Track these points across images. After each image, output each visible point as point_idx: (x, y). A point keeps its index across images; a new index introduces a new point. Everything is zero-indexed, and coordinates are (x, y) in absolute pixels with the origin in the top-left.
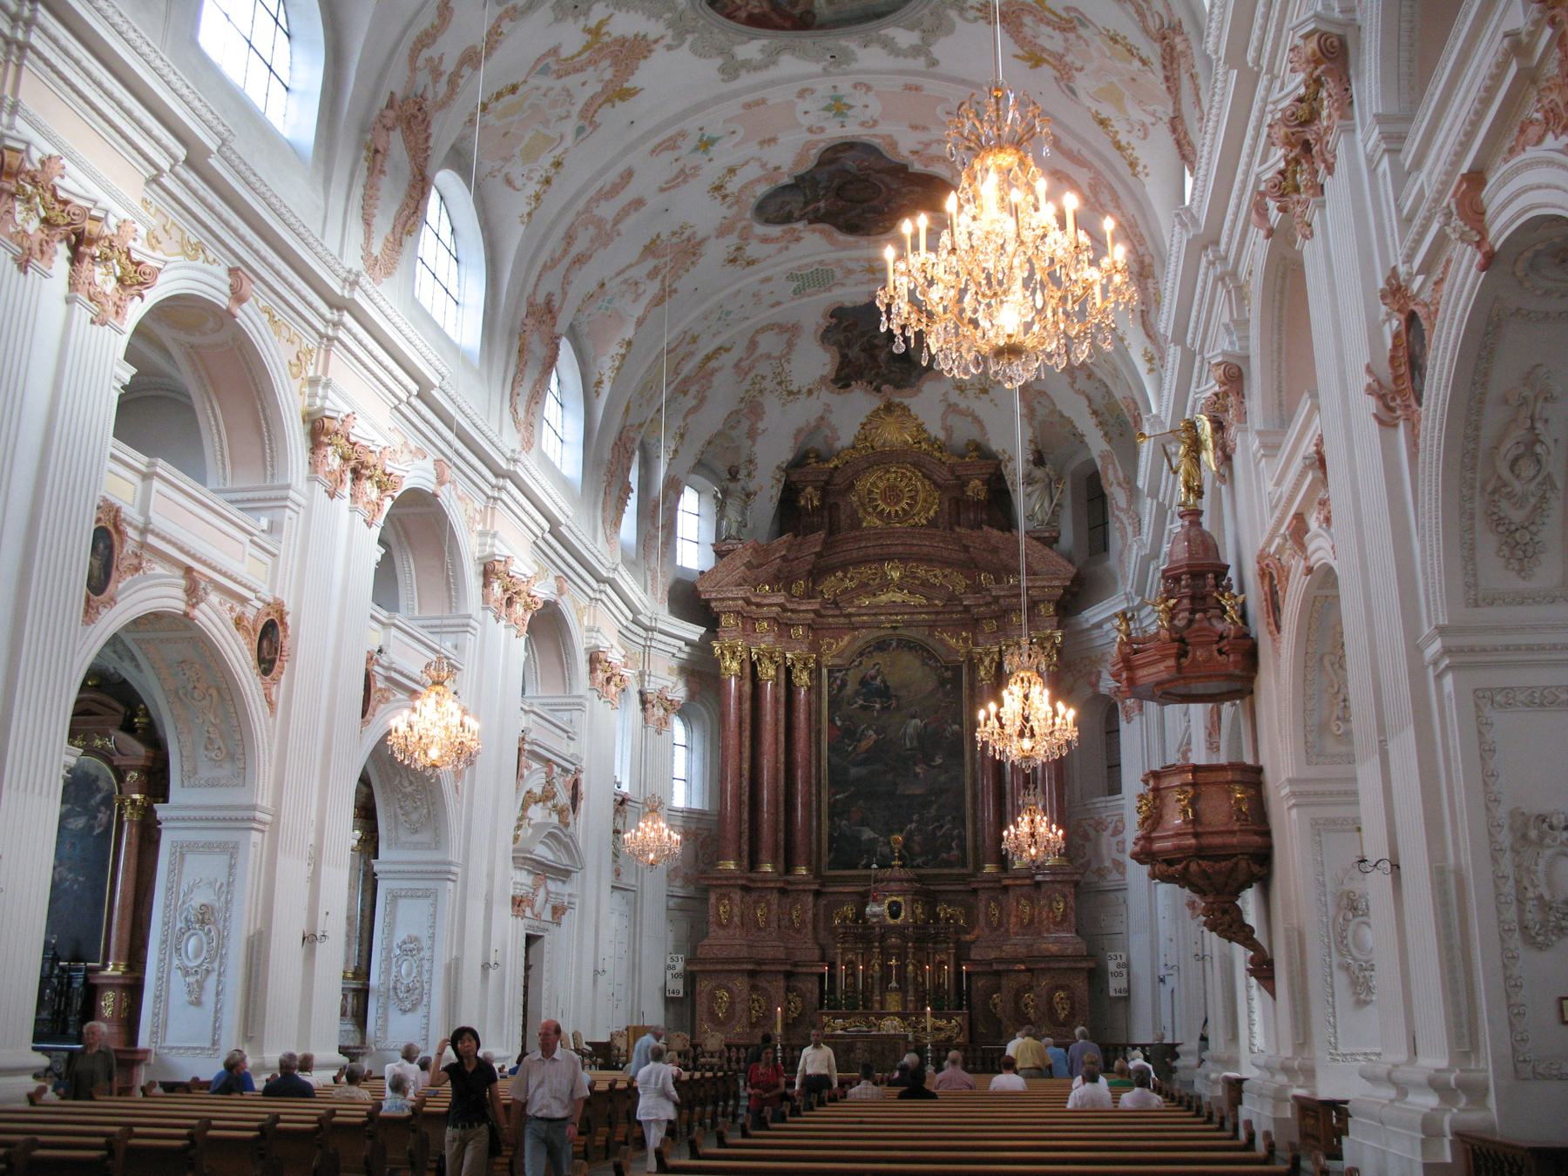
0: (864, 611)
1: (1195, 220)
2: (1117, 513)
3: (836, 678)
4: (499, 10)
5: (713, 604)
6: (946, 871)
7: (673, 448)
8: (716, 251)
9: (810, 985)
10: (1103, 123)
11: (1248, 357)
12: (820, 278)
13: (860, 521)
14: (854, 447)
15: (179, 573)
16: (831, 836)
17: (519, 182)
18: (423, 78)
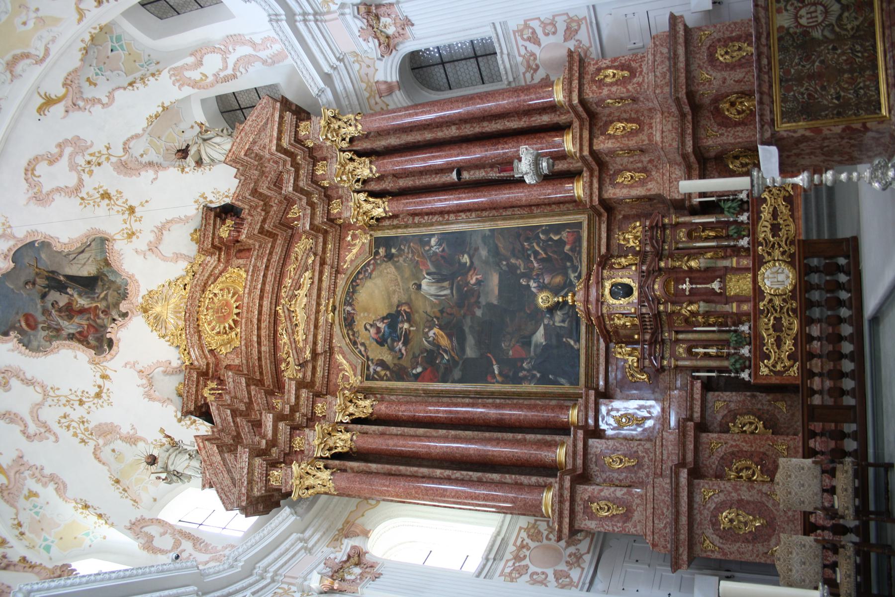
0: (311, 338)
2: (230, 71)
3: (375, 372)
5: (256, 493)
7: (95, 518)
9: (719, 404)
14: (178, 347)
16: (541, 381)
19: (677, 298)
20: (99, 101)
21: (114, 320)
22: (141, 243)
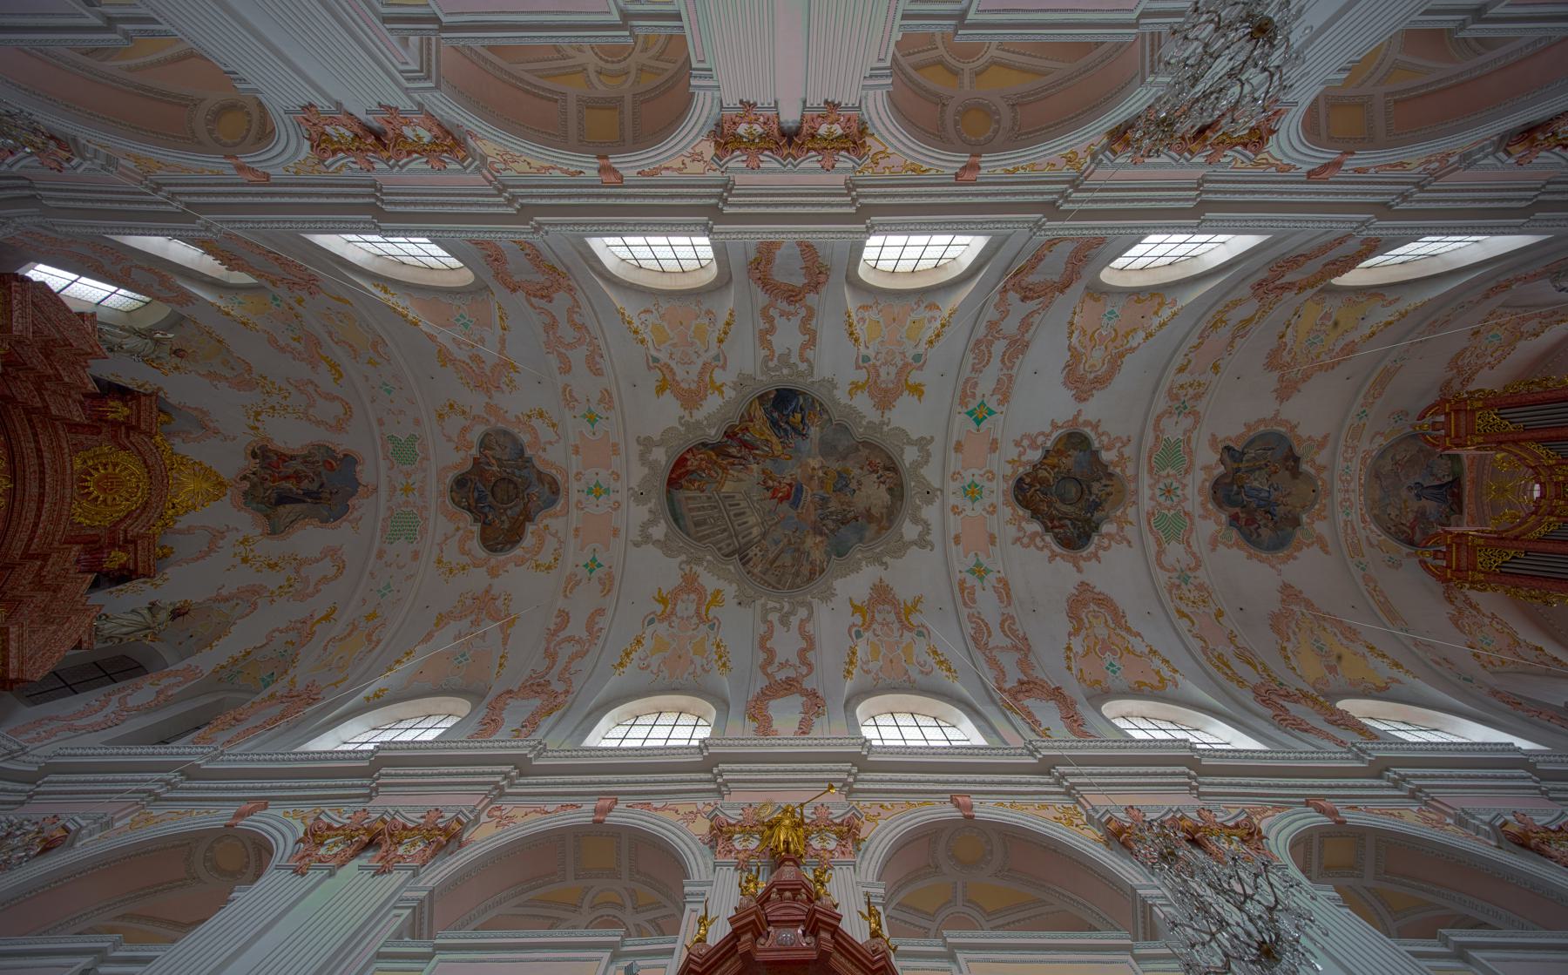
2: (115, 698)
7: (232, 313)
10: (639, 642)
20: (281, 632)
21: (254, 474)
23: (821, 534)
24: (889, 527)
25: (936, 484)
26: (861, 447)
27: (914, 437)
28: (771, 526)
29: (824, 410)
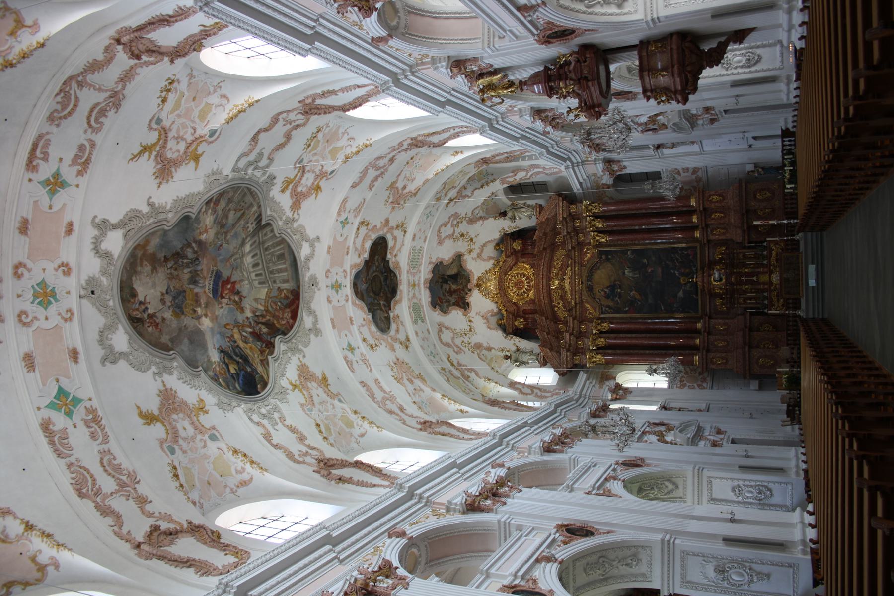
1: (386, 83)
2: (528, 177)
4: (280, 424)
6: (699, 256)
7: (494, 384)
8: (400, 352)
10: (347, 158)
11: (449, 57)
12: (416, 309)
13: (531, 300)
14: (496, 303)
15: (538, 565)
16: (682, 312)
17: (363, 431)
18: (308, 459)
19: (741, 283)
22: (474, 255)
23: (200, 243)
24: (135, 248)
25: (85, 302)
26: (170, 344)
27: (122, 363)
28: (237, 253)
29: (215, 379)
